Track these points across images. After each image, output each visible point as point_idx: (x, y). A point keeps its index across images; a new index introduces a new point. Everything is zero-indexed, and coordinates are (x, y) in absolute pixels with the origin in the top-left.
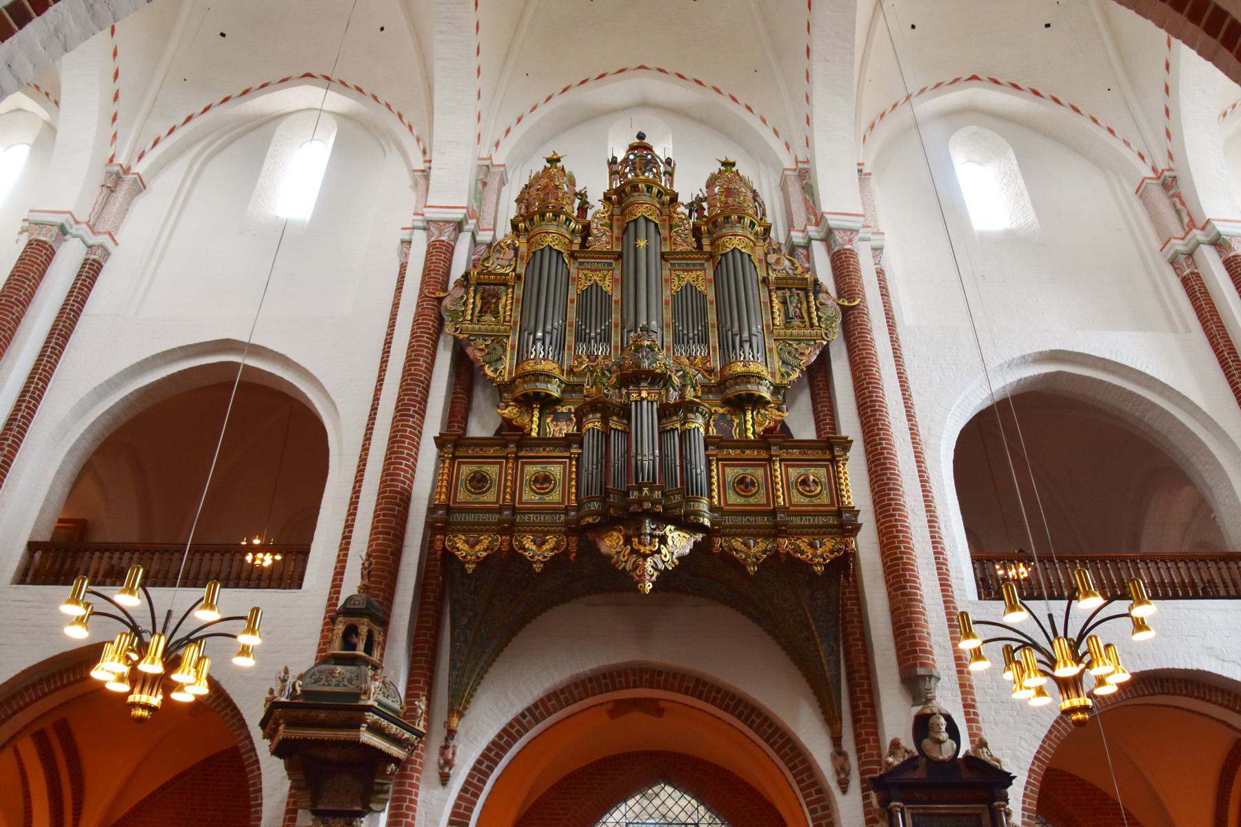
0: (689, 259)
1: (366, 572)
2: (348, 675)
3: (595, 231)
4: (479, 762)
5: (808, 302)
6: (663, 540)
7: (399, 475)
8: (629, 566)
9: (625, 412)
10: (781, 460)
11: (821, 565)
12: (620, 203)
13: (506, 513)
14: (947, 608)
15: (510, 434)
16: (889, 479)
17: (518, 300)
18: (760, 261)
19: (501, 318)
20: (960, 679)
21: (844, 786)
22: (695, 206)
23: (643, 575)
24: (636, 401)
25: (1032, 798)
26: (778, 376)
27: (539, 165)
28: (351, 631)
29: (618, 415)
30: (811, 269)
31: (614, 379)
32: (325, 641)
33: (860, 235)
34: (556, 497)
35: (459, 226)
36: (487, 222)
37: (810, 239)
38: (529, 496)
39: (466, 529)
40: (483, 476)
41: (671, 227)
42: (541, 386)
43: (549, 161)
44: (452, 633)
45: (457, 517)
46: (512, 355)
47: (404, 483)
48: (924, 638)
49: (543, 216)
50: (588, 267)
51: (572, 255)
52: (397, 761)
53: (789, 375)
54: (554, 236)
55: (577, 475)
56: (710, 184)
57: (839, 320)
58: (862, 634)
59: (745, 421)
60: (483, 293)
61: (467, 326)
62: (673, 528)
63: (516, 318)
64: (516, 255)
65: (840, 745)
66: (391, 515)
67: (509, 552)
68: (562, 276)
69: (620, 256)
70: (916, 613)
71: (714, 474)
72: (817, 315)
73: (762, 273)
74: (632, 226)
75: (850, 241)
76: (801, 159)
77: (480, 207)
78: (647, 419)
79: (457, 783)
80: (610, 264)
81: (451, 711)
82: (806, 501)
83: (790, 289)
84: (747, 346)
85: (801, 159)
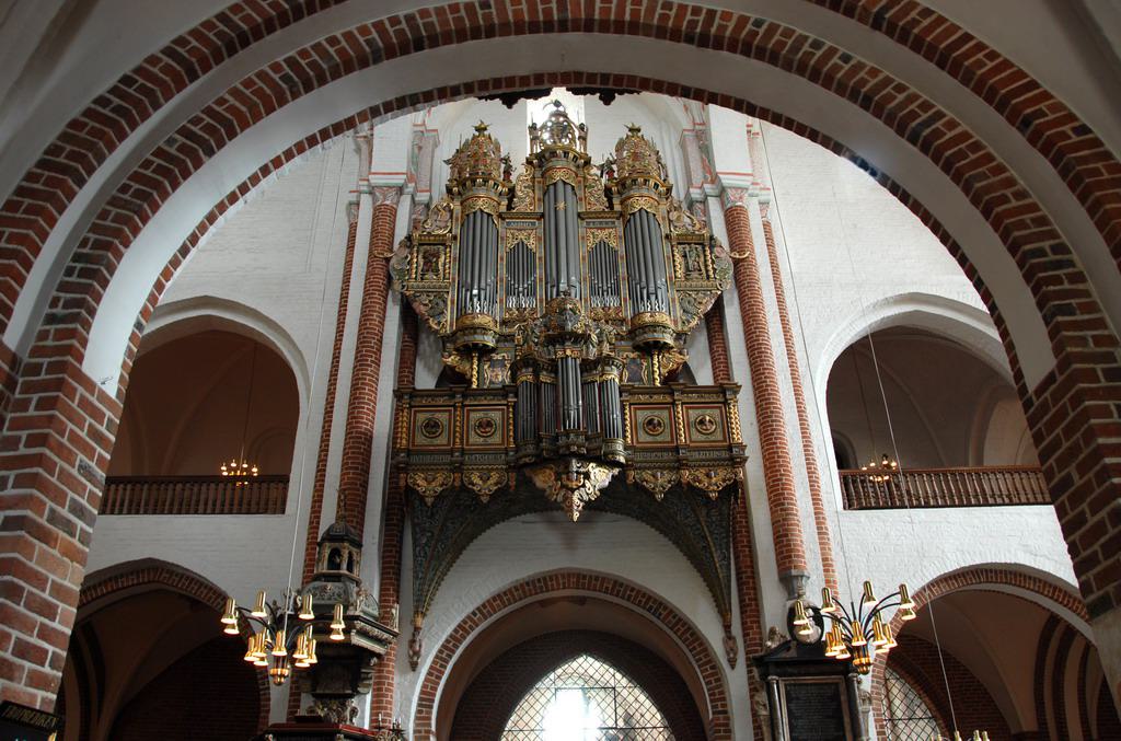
0: (602, 218)
1: (342, 504)
2: (337, 591)
3: (519, 194)
4: (440, 651)
5: (705, 256)
6: (587, 476)
7: (362, 418)
8: (560, 499)
9: (554, 367)
10: (683, 403)
11: (715, 491)
12: (540, 166)
13: (457, 454)
14: (816, 518)
15: (452, 380)
16: (772, 412)
17: (455, 258)
18: (663, 219)
19: (442, 276)
20: (825, 576)
21: (732, 663)
22: (606, 168)
23: (571, 506)
24: (562, 358)
25: (881, 668)
26: (680, 324)
27: (470, 133)
28: (335, 553)
29: (547, 370)
30: (707, 224)
31: (542, 339)
32: (310, 562)
33: (750, 192)
34: (497, 439)
35: (400, 190)
36: (423, 185)
37: (706, 196)
38: (474, 439)
39: (425, 468)
40: (436, 423)
41: (585, 187)
42: (478, 338)
43: (477, 129)
44: (414, 550)
45: (414, 459)
46: (452, 309)
47: (367, 424)
48: (798, 545)
49: (474, 181)
50: (514, 226)
51: (500, 216)
52: (379, 656)
53: (689, 322)
54: (484, 200)
55: (514, 420)
56: (620, 146)
57: (731, 272)
58: (749, 541)
59: (653, 365)
60: (425, 253)
61: (412, 283)
62: (594, 465)
63: (454, 274)
64: (451, 217)
65: (730, 632)
66: (358, 453)
67: (460, 487)
68: (493, 237)
69: (543, 215)
70: (792, 525)
71: (627, 417)
72: (713, 268)
73: (665, 231)
74: (552, 187)
75: (741, 198)
76: (698, 121)
77: (416, 170)
78: (573, 376)
79: (424, 670)
80: (533, 224)
81: (416, 612)
82: (702, 438)
83: (689, 244)
84: (653, 297)
85: (698, 121)
